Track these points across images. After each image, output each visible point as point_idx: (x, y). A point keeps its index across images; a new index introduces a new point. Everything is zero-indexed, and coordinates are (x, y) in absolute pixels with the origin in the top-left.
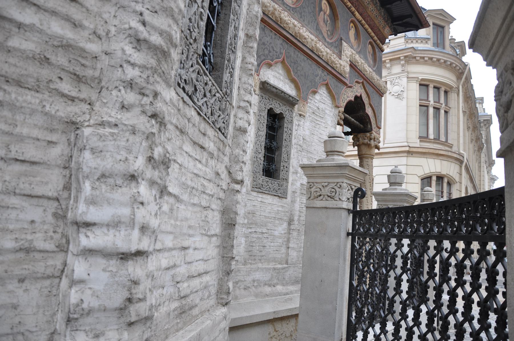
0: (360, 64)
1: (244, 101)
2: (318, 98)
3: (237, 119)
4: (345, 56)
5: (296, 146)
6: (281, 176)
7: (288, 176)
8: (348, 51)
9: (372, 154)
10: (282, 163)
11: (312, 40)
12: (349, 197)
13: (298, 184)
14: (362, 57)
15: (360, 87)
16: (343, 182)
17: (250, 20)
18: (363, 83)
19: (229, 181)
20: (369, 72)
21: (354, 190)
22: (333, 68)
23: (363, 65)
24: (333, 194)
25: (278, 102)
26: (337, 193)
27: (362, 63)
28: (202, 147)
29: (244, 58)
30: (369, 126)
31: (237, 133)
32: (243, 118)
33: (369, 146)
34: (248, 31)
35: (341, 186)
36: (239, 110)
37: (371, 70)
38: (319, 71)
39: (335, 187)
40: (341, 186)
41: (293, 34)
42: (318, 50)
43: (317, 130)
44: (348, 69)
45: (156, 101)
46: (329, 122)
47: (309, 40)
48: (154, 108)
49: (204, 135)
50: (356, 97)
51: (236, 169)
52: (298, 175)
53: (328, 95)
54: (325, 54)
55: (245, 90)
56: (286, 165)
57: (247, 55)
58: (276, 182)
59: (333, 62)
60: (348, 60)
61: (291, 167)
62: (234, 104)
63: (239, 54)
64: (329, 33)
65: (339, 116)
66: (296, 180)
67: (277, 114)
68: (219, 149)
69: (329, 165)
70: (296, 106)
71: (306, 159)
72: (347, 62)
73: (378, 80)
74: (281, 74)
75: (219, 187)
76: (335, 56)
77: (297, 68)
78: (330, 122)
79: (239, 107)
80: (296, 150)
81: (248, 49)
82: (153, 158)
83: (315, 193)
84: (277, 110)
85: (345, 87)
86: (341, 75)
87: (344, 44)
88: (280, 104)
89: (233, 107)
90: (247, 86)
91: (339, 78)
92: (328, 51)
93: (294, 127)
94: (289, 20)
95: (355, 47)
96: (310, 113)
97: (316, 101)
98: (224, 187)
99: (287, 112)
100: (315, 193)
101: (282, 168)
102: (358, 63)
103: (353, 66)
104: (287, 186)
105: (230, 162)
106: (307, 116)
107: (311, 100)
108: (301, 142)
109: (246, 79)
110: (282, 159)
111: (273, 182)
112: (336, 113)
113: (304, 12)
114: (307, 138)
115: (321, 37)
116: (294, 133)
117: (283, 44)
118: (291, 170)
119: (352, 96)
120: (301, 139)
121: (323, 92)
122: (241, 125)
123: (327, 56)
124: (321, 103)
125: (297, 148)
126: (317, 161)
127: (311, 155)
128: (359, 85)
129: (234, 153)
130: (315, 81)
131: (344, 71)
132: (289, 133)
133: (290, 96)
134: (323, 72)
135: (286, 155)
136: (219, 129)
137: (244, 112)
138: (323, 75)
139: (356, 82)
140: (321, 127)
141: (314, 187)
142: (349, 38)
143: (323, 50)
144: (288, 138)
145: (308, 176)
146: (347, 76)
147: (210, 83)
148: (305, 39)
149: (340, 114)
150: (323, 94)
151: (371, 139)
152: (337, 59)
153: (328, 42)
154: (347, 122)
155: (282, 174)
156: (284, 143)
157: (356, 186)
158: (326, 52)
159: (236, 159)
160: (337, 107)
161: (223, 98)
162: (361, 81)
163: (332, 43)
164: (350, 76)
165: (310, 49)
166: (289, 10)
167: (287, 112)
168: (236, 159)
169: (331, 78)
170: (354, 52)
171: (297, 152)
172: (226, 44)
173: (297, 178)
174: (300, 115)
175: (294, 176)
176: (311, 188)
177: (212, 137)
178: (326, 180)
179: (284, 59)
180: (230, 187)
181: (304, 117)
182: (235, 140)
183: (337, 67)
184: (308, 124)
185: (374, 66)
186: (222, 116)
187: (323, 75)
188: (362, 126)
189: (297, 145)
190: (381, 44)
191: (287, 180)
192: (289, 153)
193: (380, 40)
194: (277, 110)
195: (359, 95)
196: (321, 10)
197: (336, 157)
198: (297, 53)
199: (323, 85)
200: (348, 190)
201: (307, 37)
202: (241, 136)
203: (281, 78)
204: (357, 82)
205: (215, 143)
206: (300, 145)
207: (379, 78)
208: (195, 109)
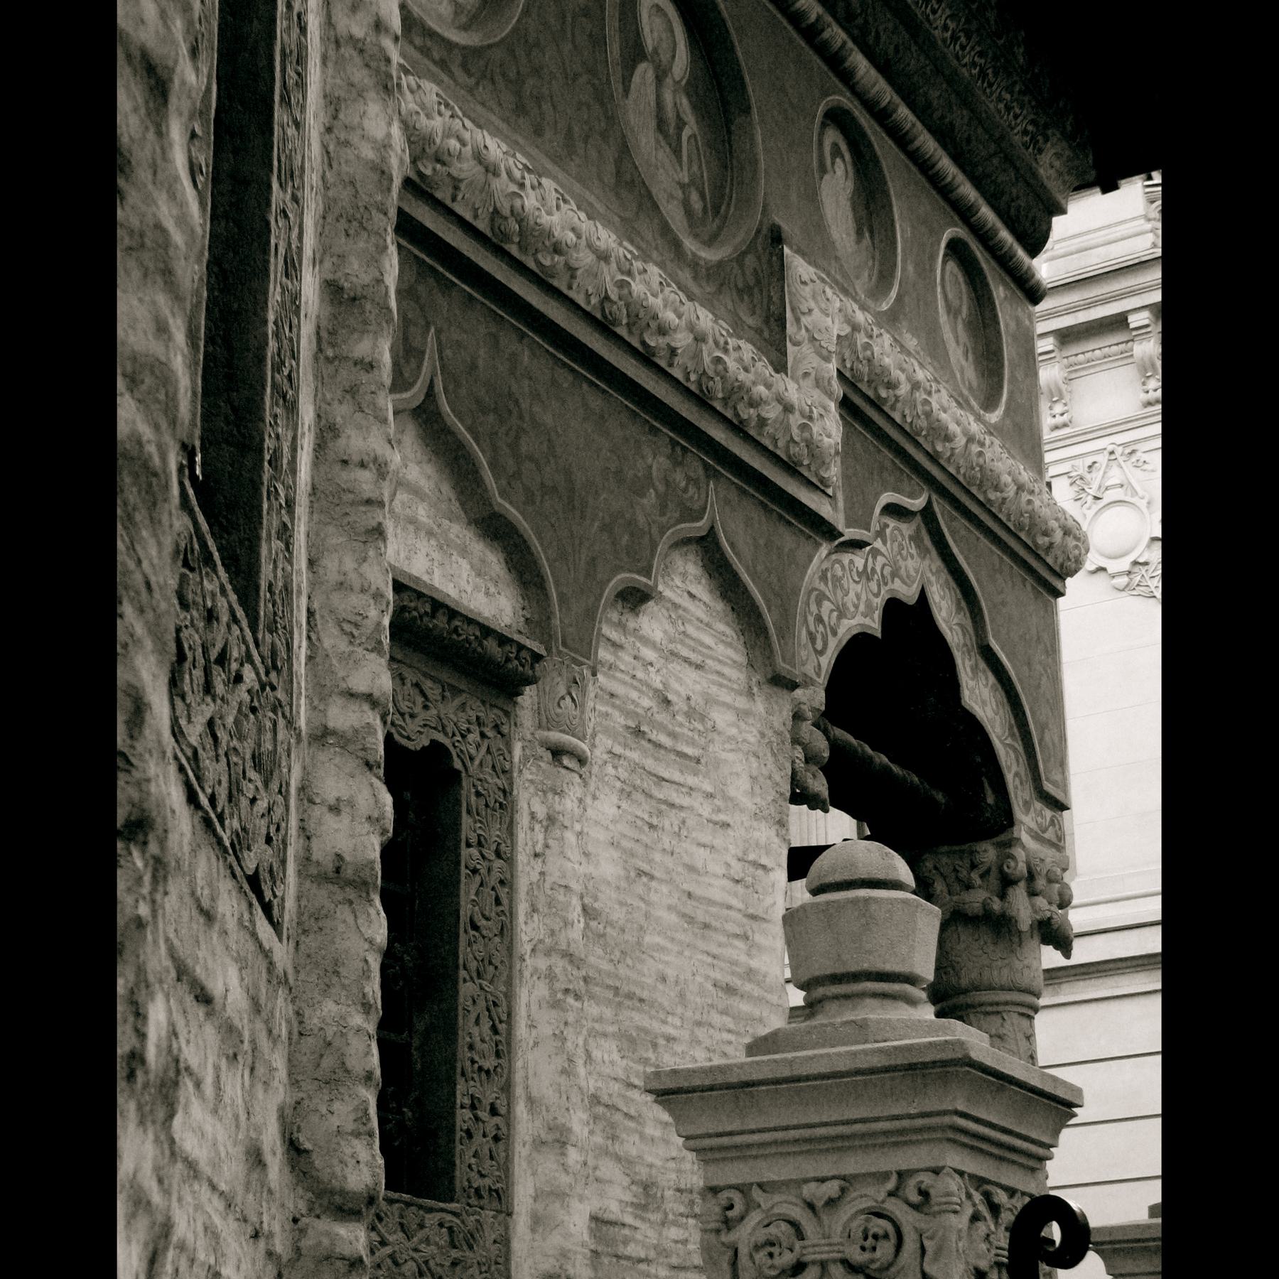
0: (904, 390)
1: (351, 695)
2: (658, 636)
3: (317, 812)
4: (806, 349)
5: (542, 963)
6: (461, 1174)
7: (506, 1169)
8: (824, 310)
9: (1024, 981)
10: (461, 1087)
11: (604, 257)
12: (983, 1265)
13: (577, 1221)
14: (911, 342)
15: (916, 539)
16: (936, 1171)
17: (345, 195)
18: (927, 514)
19: (296, 1202)
20: (960, 441)
21: (1007, 1218)
22: (738, 428)
23: (920, 396)
24: (885, 1250)
25: (411, 677)
26: (910, 1245)
27: (916, 386)
28: (204, 998)
29: (327, 432)
30: (990, 800)
31: (322, 896)
32: (351, 804)
33: (1000, 926)
34: (336, 269)
35: (924, 1194)
36: (322, 756)
37: (975, 428)
38: (654, 459)
39: (896, 1208)
40: (924, 1194)
41: (482, 225)
42: (640, 316)
43: (666, 841)
44: (830, 430)
45: (139, 747)
46: (739, 788)
47: (584, 259)
48: (138, 784)
49: (208, 916)
50: (893, 608)
51: (335, 1122)
52: (573, 1156)
53: (720, 606)
54: (682, 340)
55: (350, 627)
56: (489, 1094)
57: (341, 412)
58: (431, 1219)
59: (736, 392)
60: (832, 367)
61: (521, 1109)
62: (302, 723)
63: (307, 413)
64: (697, 205)
65: (796, 741)
66: (559, 1195)
67: (416, 752)
68: (256, 1007)
69: (842, 1066)
70: (528, 697)
71: (611, 1045)
72: (818, 383)
73: (1020, 488)
74: (416, 491)
75: (262, 1244)
76: (748, 350)
77: (514, 446)
78: (744, 784)
79: (322, 736)
80: (542, 990)
81: (346, 375)
82: (143, 1061)
83: (761, 1256)
84: (412, 727)
85: (824, 549)
86: (791, 468)
87: (799, 267)
88: (427, 684)
89: (299, 736)
90: (356, 600)
91: (773, 490)
92: (705, 319)
93: (521, 836)
94: (448, 133)
95: (861, 286)
96: (613, 735)
97: (649, 654)
98: (279, 1248)
99: (474, 737)
100: (761, 1256)
101: (463, 1117)
102: (891, 385)
103: (862, 406)
104: (504, 1242)
105: (294, 1083)
106: (598, 755)
107: (617, 646)
108: (576, 933)
109: (349, 564)
110: (463, 1054)
111: (412, 1216)
112: (777, 724)
113: (537, 71)
114: (607, 901)
115: (648, 231)
116: (526, 872)
117: (421, 288)
118: (525, 1126)
119: (870, 609)
120: (575, 913)
121: (684, 584)
122: (344, 844)
123: (697, 356)
124: (676, 666)
125: (551, 976)
126: (751, 1049)
127: (640, 1019)
128: (907, 529)
129: (313, 1022)
130: (631, 523)
131: (809, 444)
132: (493, 880)
133: (487, 631)
134: (677, 464)
135: (486, 1025)
136: (254, 881)
137: (352, 764)
138: (679, 477)
139: (893, 510)
140: (691, 822)
141: (755, 1218)
142: (818, 226)
143: (669, 316)
144: (491, 910)
145: (707, 1150)
146: (834, 472)
147: (222, 603)
148: (557, 249)
149: (807, 729)
150: (685, 602)
151: (1007, 882)
152: (764, 368)
153: (694, 265)
154: (848, 786)
155: (467, 1161)
156: (468, 952)
157: (1012, 1192)
158: (691, 328)
159: (327, 1062)
160: (783, 682)
161: (263, 689)
162: (917, 503)
163: (720, 264)
164: (846, 477)
165: (587, 316)
166: (443, 64)
167: (474, 737)
168: (327, 1062)
169: (733, 495)
170: (860, 317)
171: (556, 1005)
172: (261, 360)
173: (565, 1179)
174: (557, 752)
175: (548, 1164)
176: (728, 1224)
177: (231, 924)
178: (826, 1166)
179: (430, 393)
180: (306, 1243)
181: (582, 761)
182: (310, 942)
183: (762, 422)
184: (606, 806)
185: (990, 402)
186: (262, 805)
187: (679, 477)
188: (940, 797)
189: (548, 953)
190: (1021, 253)
191: (500, 1197)
192: (502, 1010)
193: (1013, 231)
194: (412, 727)
195: (909, 594)
196: (635, 52)
197: (873, 1012)
198: (509, 343)
199: (683, 543)
200: (975, 1218)
201: (571, 237)
202: (344, 913)
203: (422, 512)
204: (893, 510)
205: (243, 964)
206: (568, 956)
207: (1026, 476)
208: (181, 769)
